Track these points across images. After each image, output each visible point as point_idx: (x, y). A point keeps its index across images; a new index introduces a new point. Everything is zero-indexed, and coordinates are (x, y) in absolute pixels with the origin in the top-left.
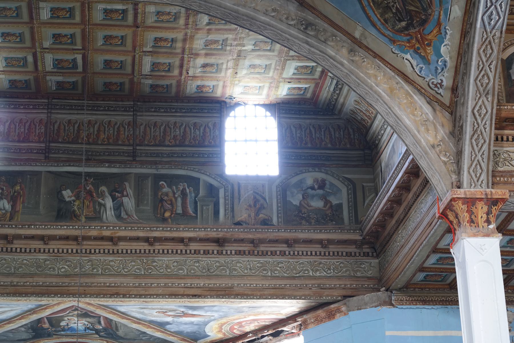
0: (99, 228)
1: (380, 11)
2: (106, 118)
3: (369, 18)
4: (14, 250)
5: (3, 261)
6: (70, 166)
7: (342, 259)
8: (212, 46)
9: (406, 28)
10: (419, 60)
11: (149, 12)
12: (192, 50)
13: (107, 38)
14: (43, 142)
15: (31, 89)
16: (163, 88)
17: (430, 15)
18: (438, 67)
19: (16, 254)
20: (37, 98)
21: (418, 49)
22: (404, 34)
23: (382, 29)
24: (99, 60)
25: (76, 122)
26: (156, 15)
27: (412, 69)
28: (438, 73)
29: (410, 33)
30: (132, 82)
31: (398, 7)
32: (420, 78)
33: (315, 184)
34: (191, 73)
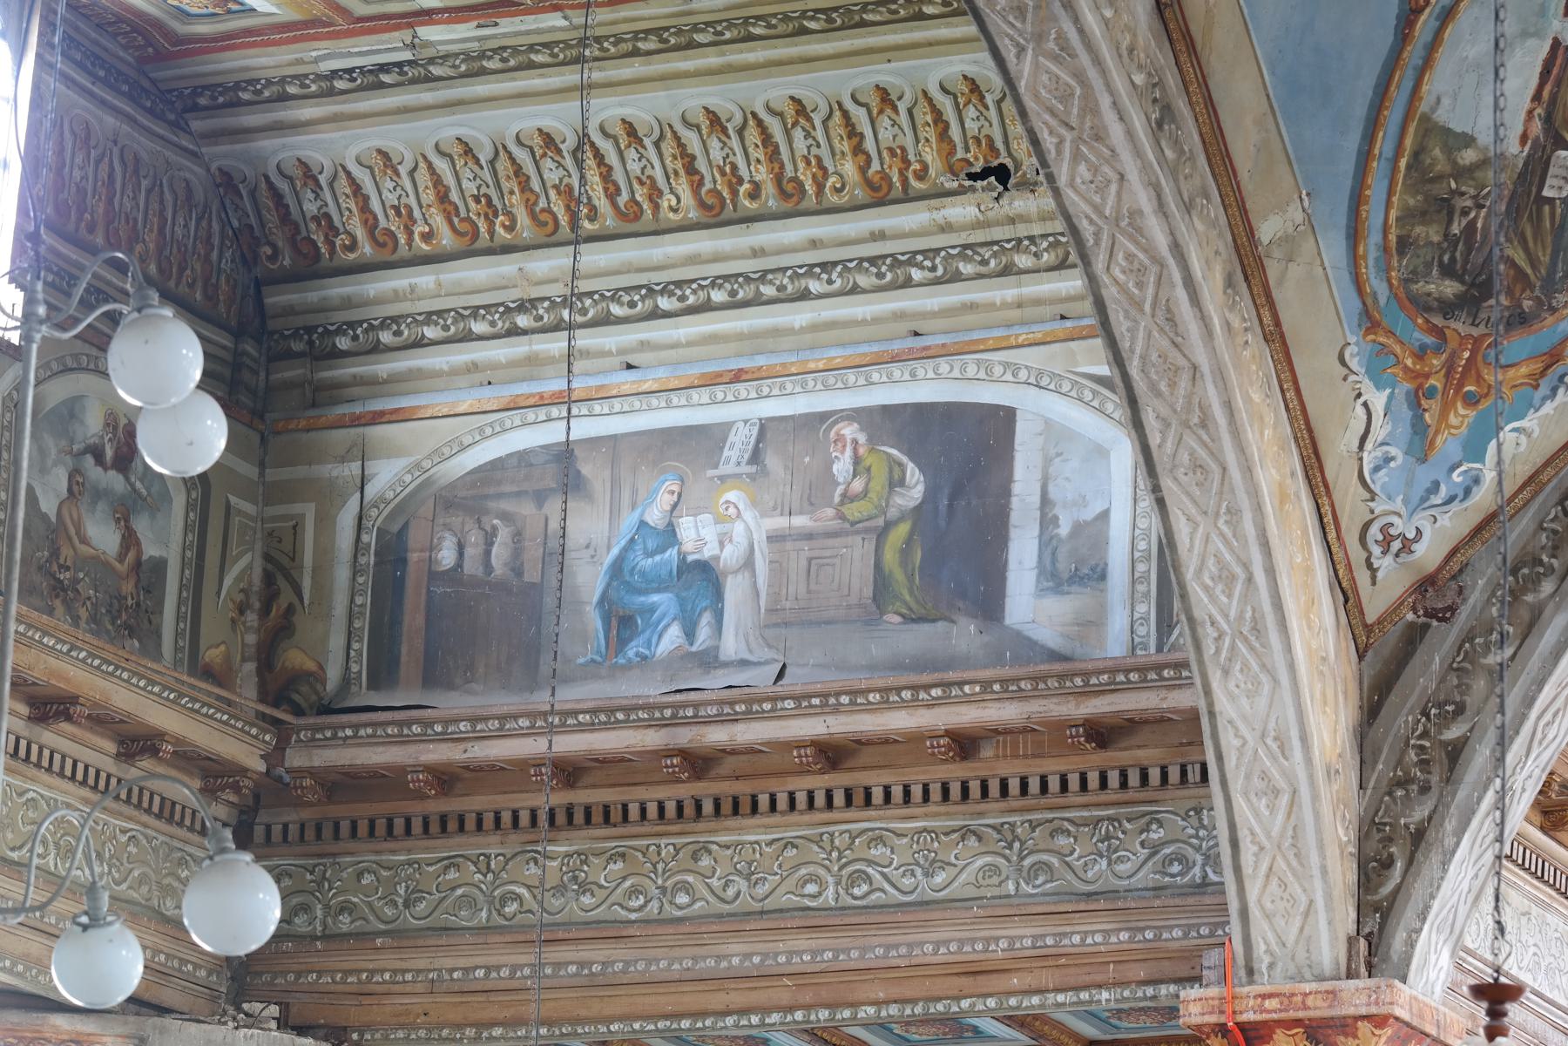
1: (1411, 202)
3: (1357, 200)
7: (138, 822)
9: (1448, 308)
10: (1404, 430)
17: (1553, 310)
18: (1443, 488)
21: (1431, 393)
22: (1427, 321)
23: (1371, 262)
27: (1356, 443)
28: (1426, 505)
29: (1447, 332)
31: (1479, 225)
32: (1361, 490)
33: (106, 439)
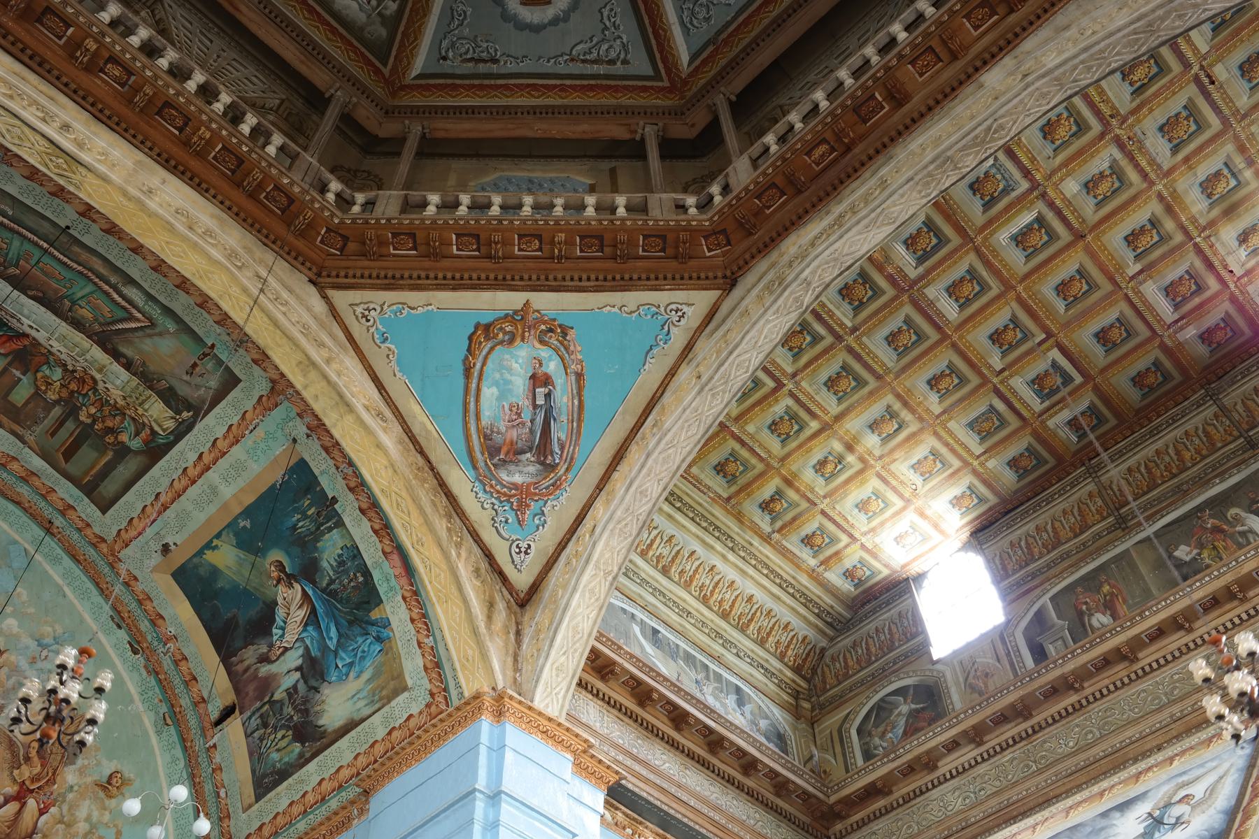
0: (1253, 553)
2: (1179, 433)
4: (1147, 669)
5: (1142, 695)
6: (1163, 516)
8: (1219, 190)
11: (1074, 196)
12: (1196, 220)
13: (1062, 289)
14: (1109, 515)
15: (1047, 462)
16: (1222, 328)
19: (1155, 673)
20: (1069, 474)
24: (1085, 338)
25: (1139, 464)
26: (1088, 193)
30: (1164, 348)
34: (1238, 272)
